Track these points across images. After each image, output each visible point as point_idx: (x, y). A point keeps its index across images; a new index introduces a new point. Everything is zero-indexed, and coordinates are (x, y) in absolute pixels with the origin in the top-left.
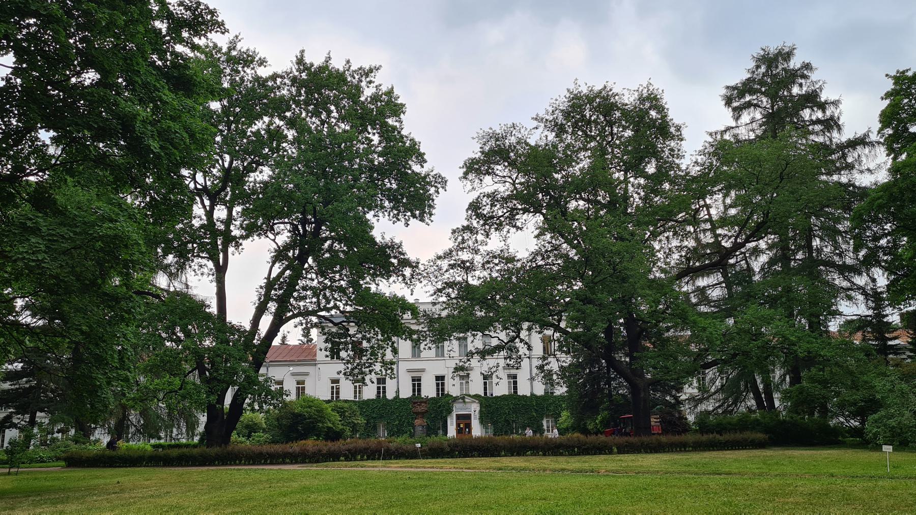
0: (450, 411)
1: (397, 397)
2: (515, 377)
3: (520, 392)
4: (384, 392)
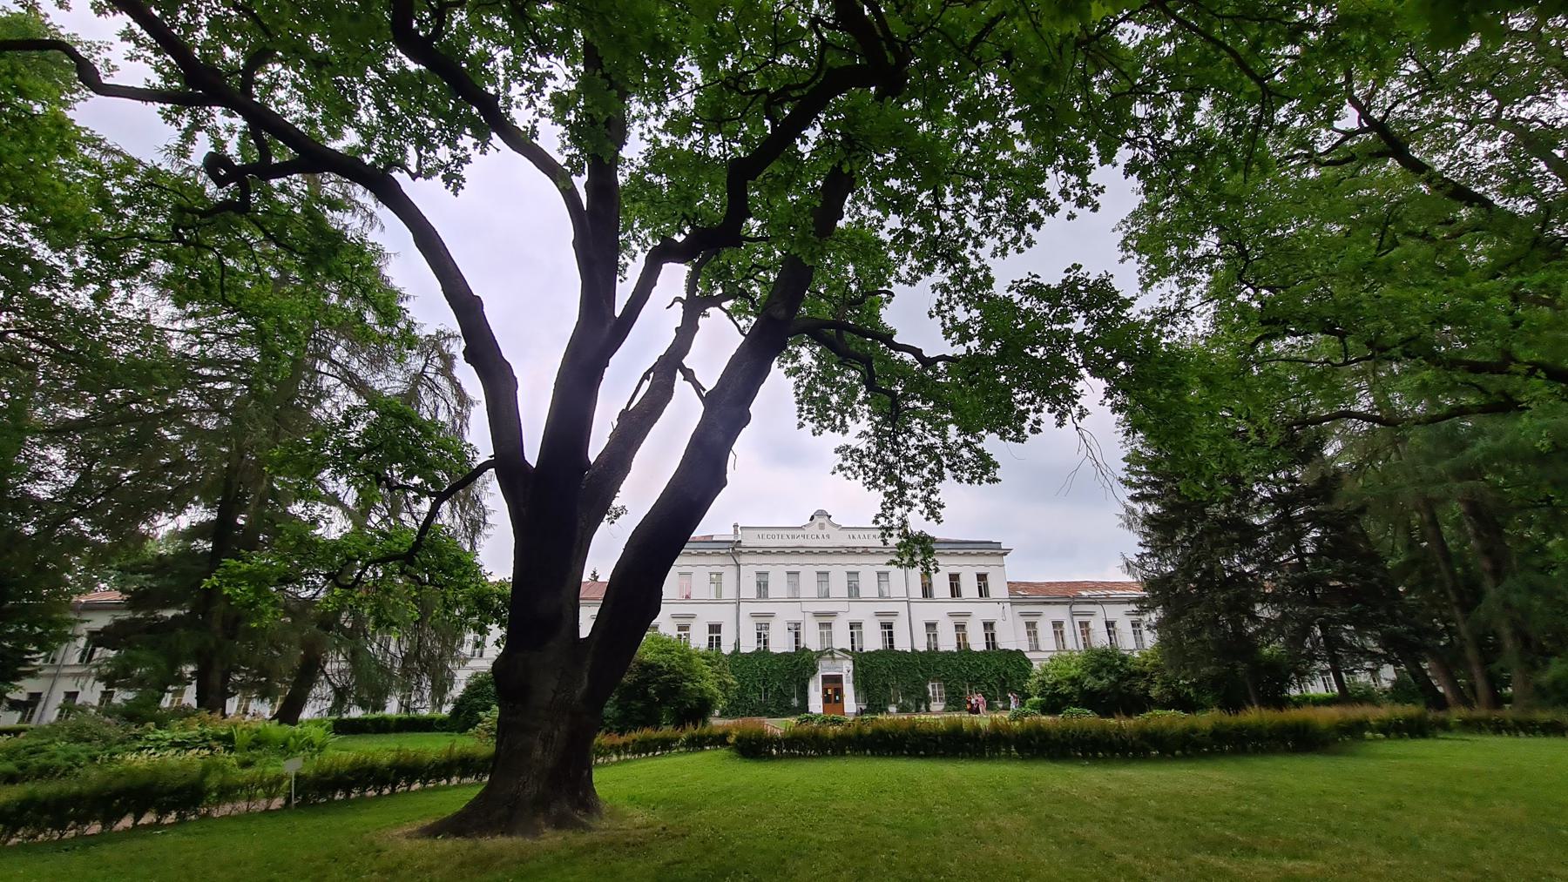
0: (814, 671)
1: (736, 651)
2: (890, 626)
3: (898, 646)
4: (719, 644)
